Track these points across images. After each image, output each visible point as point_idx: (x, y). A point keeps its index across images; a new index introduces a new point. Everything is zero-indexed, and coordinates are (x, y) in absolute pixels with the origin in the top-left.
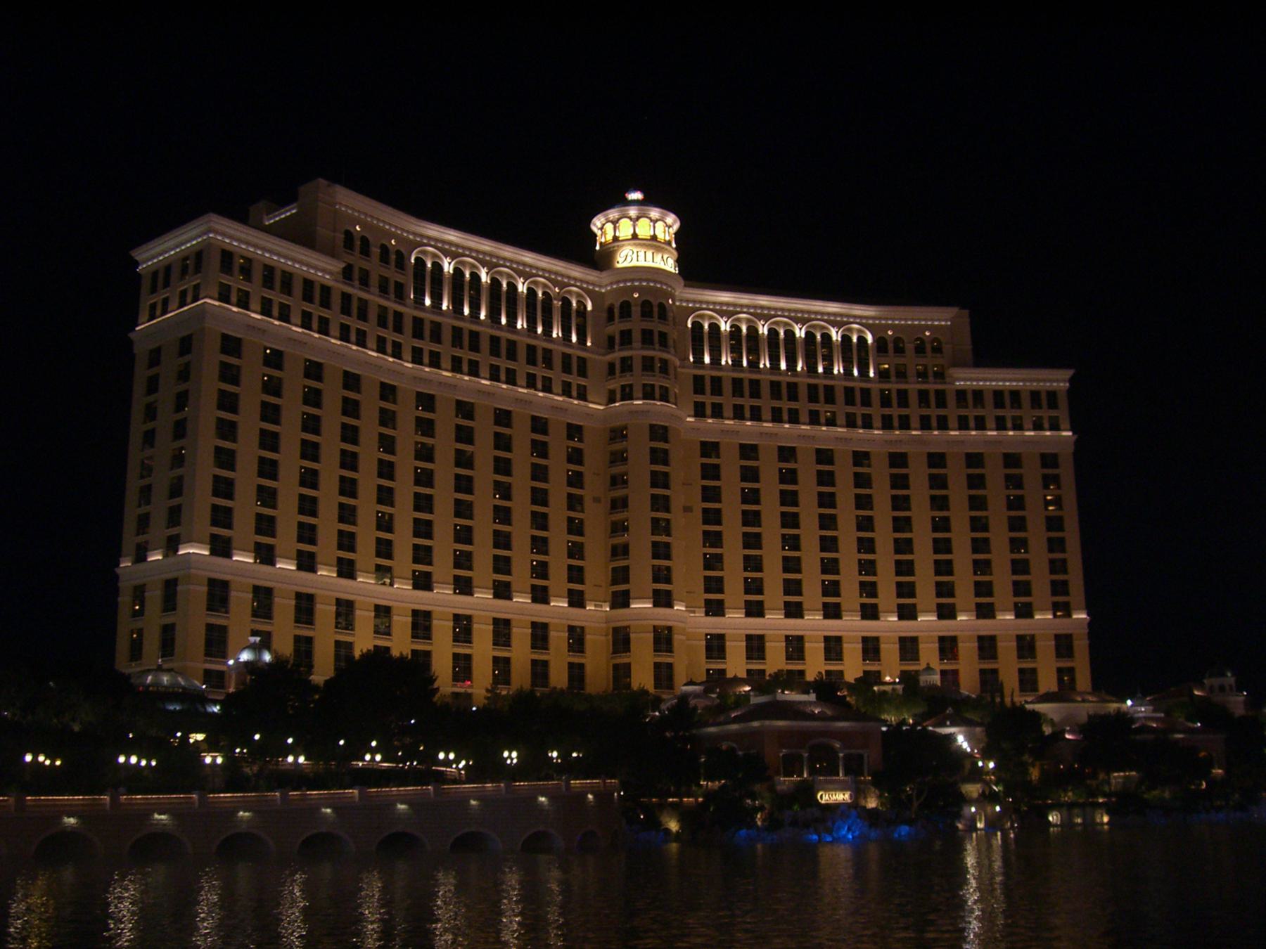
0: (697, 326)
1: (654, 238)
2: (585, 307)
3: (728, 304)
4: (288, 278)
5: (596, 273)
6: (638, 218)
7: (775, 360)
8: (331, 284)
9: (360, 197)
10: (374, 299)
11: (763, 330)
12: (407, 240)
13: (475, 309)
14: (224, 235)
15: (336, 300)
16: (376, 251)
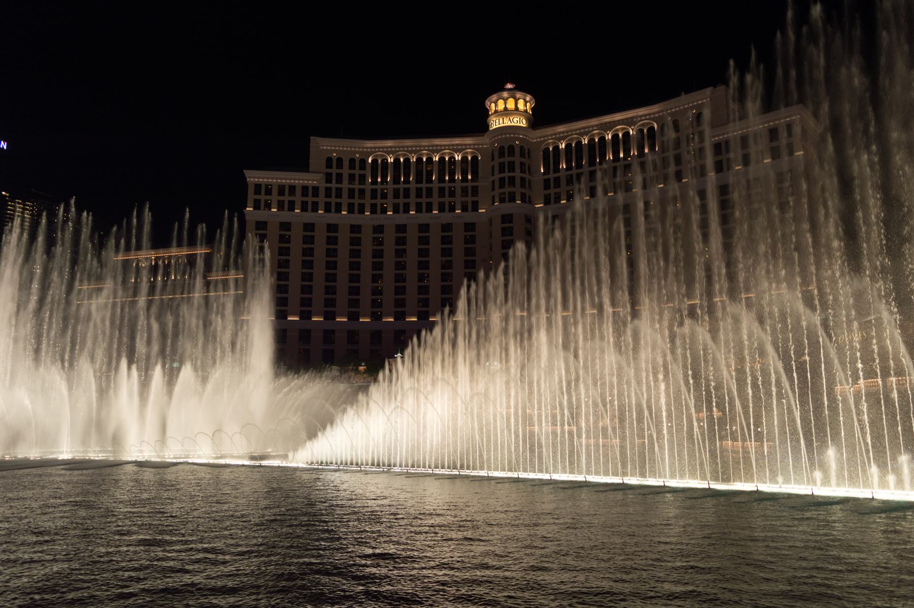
0: (546, 151)
1: (506, 109)
2: (478, 158)
3: (563, 132)
4: (292, 188)
5: (480, 138)
6: (497, 100)
7: (616, 153)
8: (318, 185)
9: (327, 139)
10: (345, 185)
11: (585, 141)
12: (367, 152)
13: (407, 176)
14: (254, 178)
15: (322, 193)
16: (346, 164)
